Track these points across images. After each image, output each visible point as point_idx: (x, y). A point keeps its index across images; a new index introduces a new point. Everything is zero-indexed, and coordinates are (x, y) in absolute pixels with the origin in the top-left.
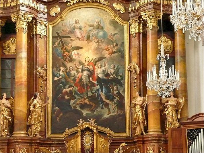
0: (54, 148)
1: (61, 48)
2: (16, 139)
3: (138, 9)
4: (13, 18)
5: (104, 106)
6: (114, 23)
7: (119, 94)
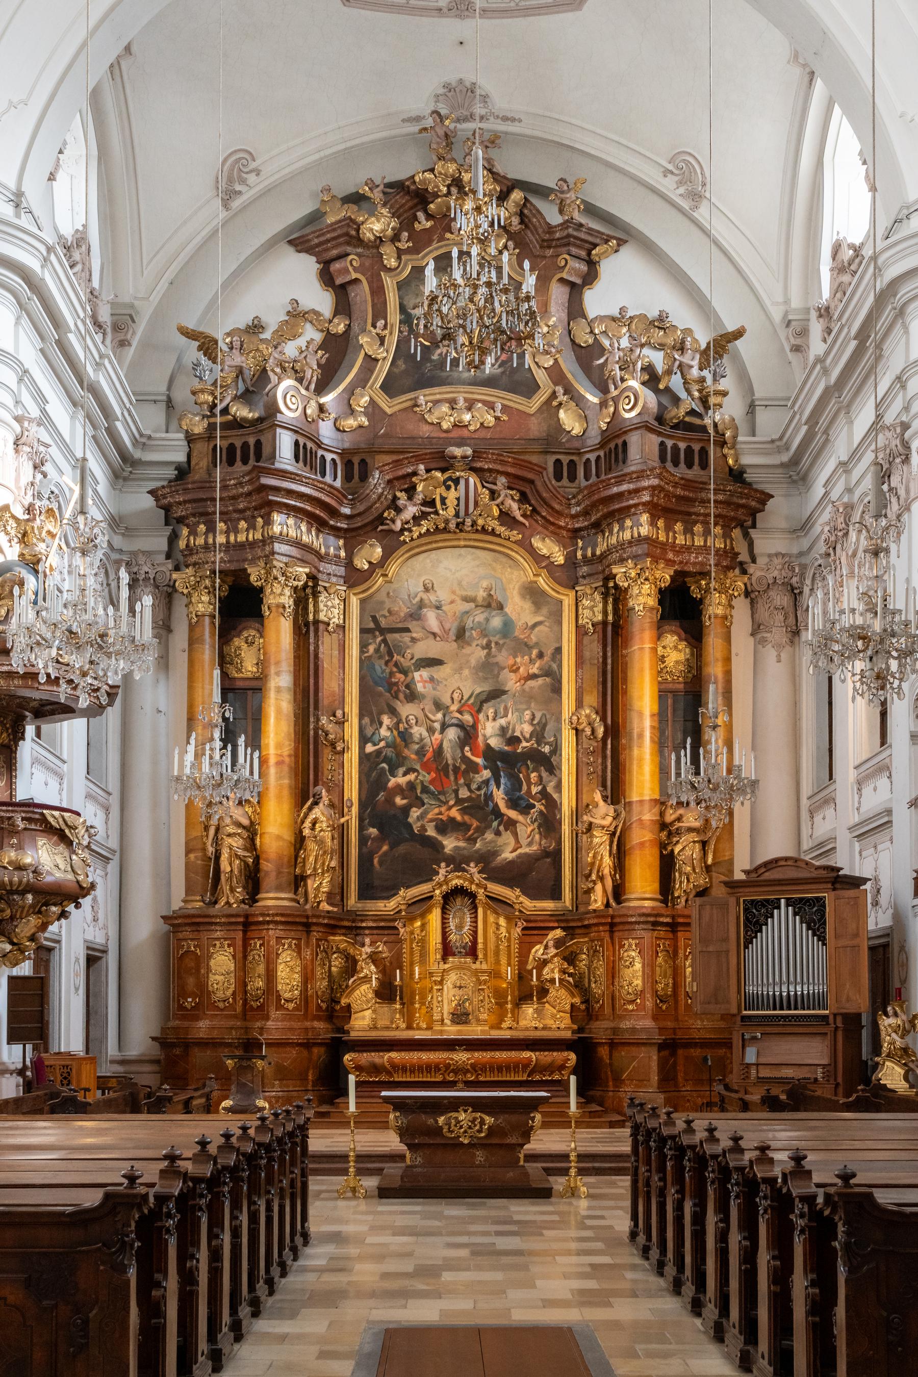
0: (367, 941)
1: (383, 662)
2: (268, 915)
3: (603, 556)
4: (255, 575)
5: (502, 828)
6: (533, 593)
7: (544, 794)
